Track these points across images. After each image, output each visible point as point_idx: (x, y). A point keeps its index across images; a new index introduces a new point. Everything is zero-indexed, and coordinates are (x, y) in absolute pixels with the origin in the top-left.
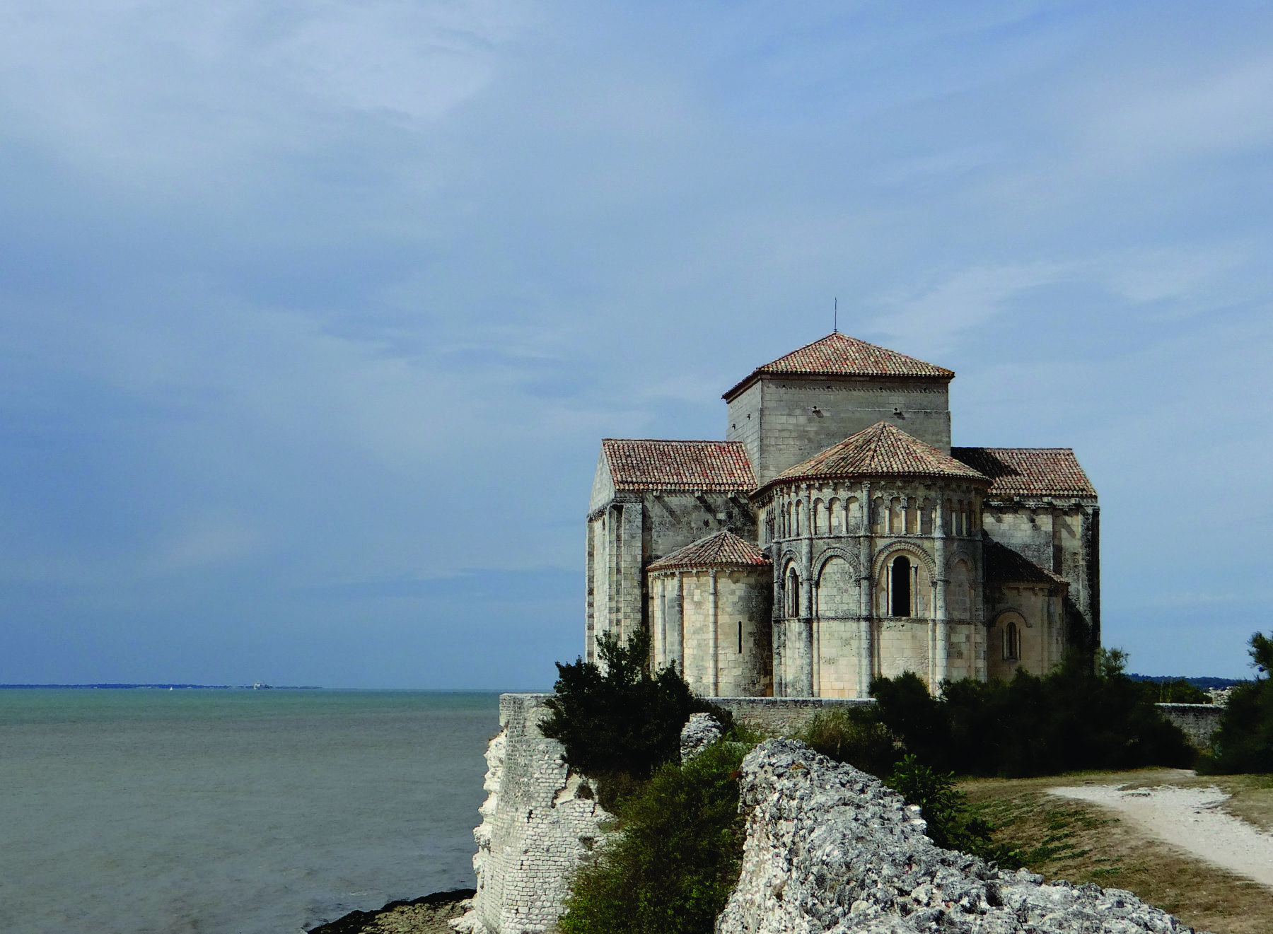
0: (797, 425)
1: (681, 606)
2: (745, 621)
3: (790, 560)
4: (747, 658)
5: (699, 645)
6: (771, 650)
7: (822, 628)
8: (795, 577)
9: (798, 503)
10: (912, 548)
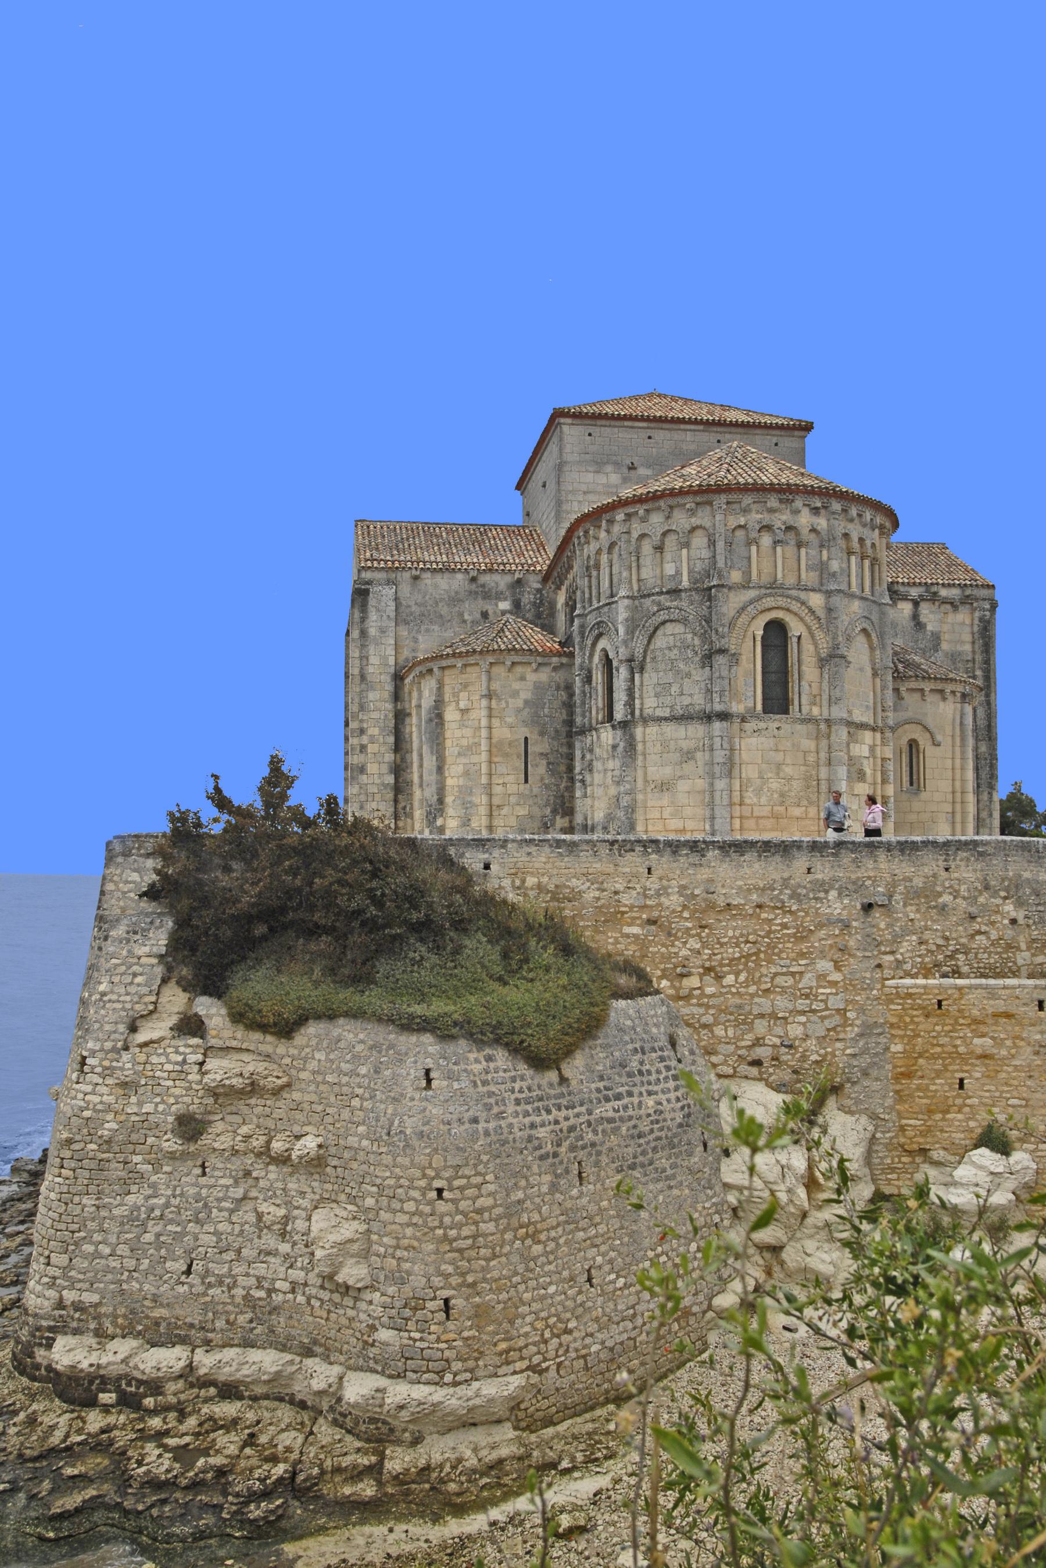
0: (608, 485)
1: (440, 716)
2: (533, 737)
3: (600, 635)
4: (536, 790)
5: (466, 774)
6: (572, 780)
7: (645, 734)
8: (608, 662)
9: (612, 546)
10: (795, 606)
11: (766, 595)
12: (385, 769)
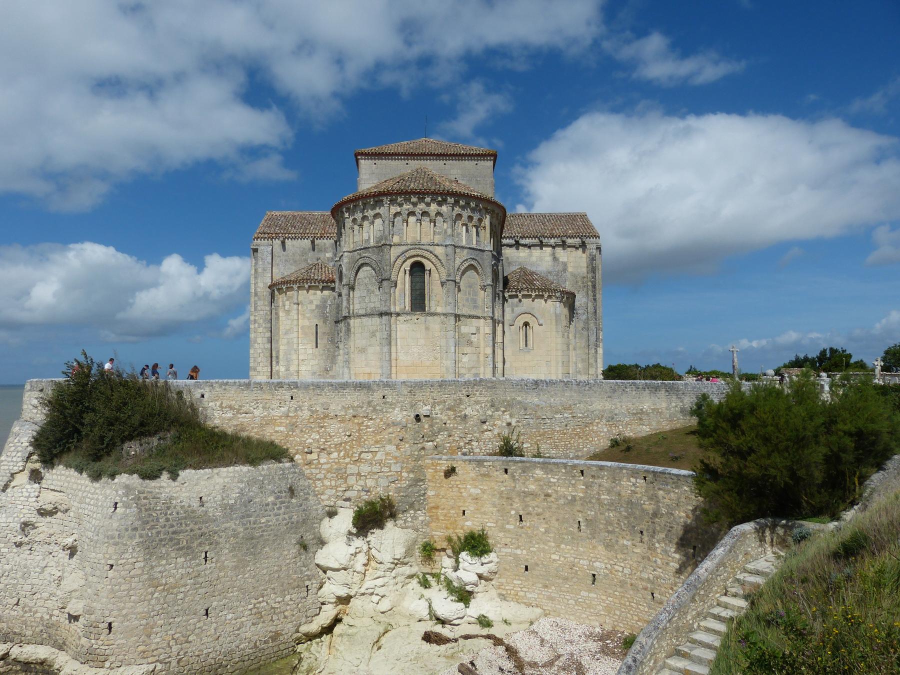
2: (320, 324)
4: (322, 352)
11: (410, 249)
12: (265, 340)
